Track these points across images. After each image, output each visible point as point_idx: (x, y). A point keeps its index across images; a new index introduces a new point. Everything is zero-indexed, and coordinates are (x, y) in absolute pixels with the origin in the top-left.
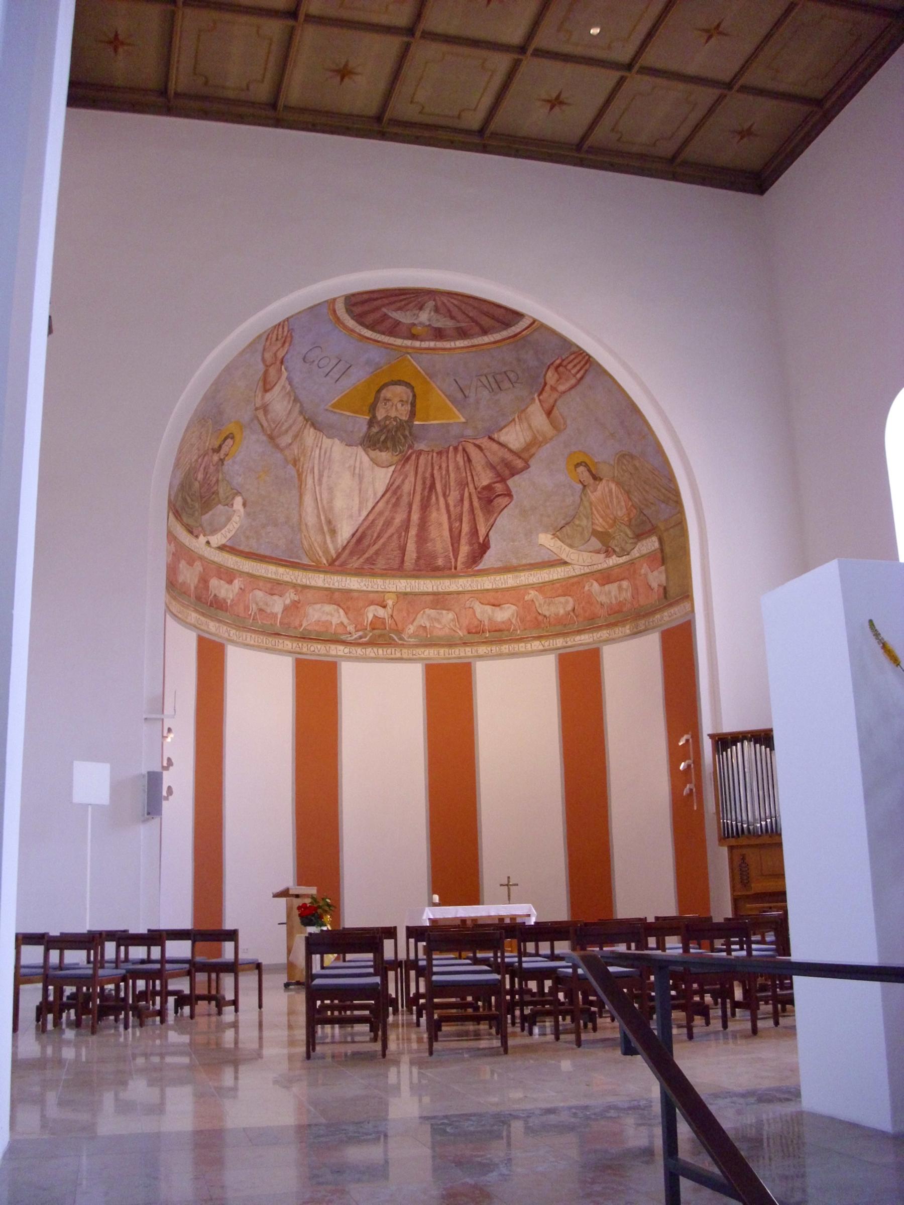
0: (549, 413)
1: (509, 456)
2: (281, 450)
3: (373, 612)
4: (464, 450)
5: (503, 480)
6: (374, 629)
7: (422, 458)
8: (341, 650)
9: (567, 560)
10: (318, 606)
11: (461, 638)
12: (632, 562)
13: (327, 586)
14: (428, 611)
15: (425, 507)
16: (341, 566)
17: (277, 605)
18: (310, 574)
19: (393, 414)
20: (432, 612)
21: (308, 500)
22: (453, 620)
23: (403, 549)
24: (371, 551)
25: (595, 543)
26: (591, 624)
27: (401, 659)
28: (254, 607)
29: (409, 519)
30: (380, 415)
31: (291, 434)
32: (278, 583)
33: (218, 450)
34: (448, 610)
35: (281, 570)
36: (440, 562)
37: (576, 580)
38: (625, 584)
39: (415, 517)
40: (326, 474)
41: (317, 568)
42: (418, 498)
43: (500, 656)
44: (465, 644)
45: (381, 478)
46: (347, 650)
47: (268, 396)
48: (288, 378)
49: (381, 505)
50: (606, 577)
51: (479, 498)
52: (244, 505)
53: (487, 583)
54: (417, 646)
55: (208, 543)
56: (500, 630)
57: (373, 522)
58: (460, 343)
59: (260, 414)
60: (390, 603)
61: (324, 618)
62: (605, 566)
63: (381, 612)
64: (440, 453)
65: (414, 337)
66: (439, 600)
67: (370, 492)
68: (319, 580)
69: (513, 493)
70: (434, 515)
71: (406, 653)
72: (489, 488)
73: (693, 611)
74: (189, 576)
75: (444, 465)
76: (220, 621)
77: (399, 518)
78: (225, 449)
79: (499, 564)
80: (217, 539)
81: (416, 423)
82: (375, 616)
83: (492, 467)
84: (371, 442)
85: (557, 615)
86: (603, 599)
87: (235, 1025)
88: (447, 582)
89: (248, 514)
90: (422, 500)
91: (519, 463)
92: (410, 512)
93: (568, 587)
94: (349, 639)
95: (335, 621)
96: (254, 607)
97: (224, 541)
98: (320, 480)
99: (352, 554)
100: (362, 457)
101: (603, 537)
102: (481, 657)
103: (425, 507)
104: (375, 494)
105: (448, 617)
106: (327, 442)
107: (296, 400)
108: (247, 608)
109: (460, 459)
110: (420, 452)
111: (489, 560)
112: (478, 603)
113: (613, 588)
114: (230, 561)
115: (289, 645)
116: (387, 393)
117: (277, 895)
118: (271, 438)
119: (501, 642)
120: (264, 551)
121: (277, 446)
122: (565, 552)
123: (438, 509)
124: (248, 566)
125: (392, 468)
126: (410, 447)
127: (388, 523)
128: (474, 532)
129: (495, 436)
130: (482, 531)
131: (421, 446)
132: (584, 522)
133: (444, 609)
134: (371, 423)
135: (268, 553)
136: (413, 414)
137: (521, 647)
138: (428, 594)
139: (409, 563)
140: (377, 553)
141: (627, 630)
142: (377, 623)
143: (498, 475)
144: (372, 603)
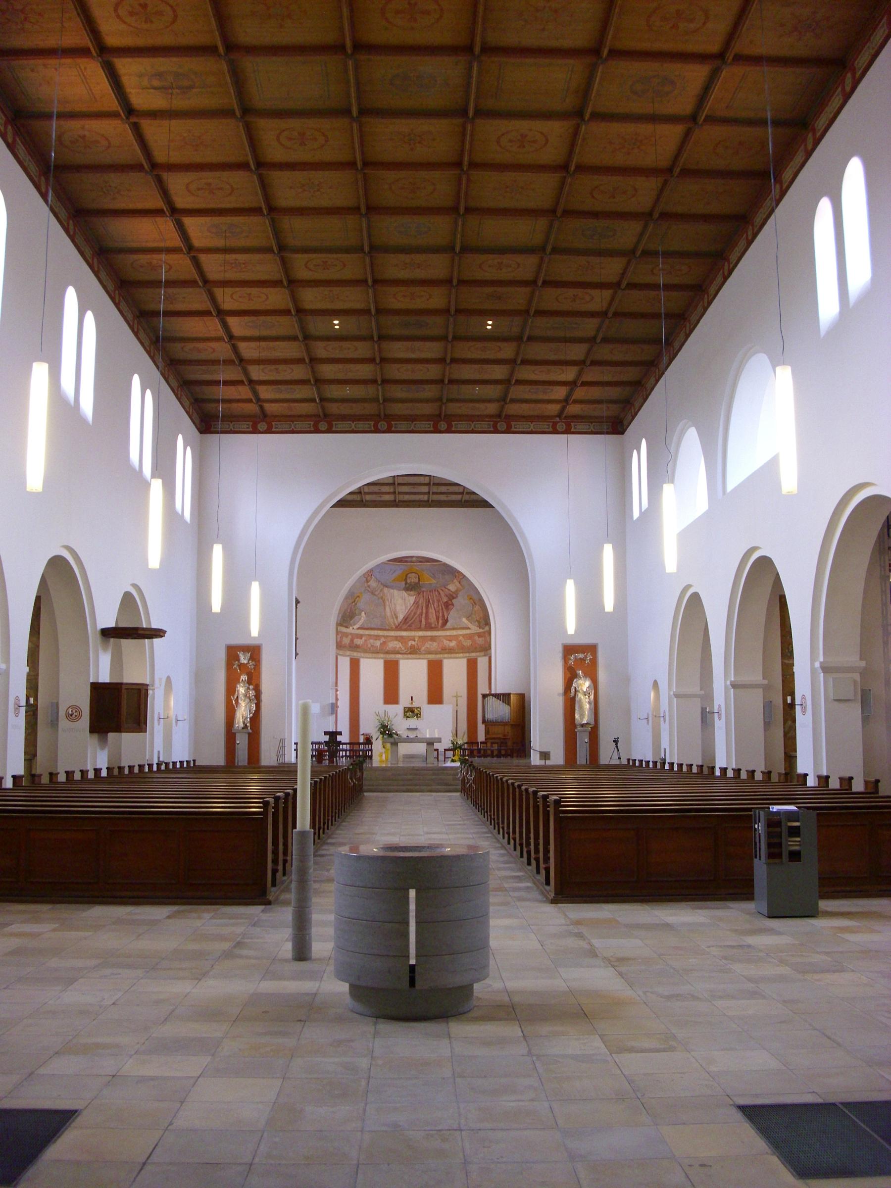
1: (451, 593)
3: (410, 643)
5: (451, 600)
8: (400, 656)
15: (427, 607)
17: (378, 643)
18: (390, 632)
19: (413, 581)
20: (429, 642)
21: (387, 609)
23: (421, 622)
24: (410, 622)
27: (420, 658)
28: (369, 645)
29: (422, 612)
30: (409, 581)
31: (379, 591)
35: (379, 632)
36: (433, 625)
38: (483, 638)
39: (424, 611)
41: (391, 629)
42: (424, 605)
43: (451, 658)
44: (441, 654)
45: (412, 599)
47: (369, 583)
49: (413, 607)
50: (479, 635)
52: (365, 614)
53: (448, 633)
54: (425, 654)
59: (368, 588)
60: (416, 640)
63: (414, 643)
64: (430, 592)
65: (413, 562)
66: (433, 639)
68: (392, 633)
71: (421, 656)
72: (446, 602)
74: (346, 641)
79: (451, 627)
80: (355, 627)
83: (447, 596)
84: (407, 589)
86: (478, 642)
91: (454, 596)
92: (422, 610)
93: (470, 637)
94: (403, 652)
95: (398, 646)
96: (369, 645)
99: (403, 624)
100: (404, 594)
101: (479, 622)
102: (445, 658)
103: (427, 607)
105: (435, 644)
106: (392, 591)
107: (379, 581)
109: (436, 592)
110: (423, 592)
111: (449, 625)
113: (481, 639)
114: (361, 632)
115: (382, 656)
116: (410, 575)
119: (452, 653)
120: (373, 626)
121: (375, 595)
122: (470, 625)
124: (367, 632)
125: (415, 597)
126: (420, 590)
127: (415, 614)
128: (443, 616)
130: (446, 617)
131: (424, 589)
132: (474, 617)
134: (406, 584)
136: (419, 580)
137: (457, 655)
140: (412, 623)
141: (482, 654)
142: (412, 647)
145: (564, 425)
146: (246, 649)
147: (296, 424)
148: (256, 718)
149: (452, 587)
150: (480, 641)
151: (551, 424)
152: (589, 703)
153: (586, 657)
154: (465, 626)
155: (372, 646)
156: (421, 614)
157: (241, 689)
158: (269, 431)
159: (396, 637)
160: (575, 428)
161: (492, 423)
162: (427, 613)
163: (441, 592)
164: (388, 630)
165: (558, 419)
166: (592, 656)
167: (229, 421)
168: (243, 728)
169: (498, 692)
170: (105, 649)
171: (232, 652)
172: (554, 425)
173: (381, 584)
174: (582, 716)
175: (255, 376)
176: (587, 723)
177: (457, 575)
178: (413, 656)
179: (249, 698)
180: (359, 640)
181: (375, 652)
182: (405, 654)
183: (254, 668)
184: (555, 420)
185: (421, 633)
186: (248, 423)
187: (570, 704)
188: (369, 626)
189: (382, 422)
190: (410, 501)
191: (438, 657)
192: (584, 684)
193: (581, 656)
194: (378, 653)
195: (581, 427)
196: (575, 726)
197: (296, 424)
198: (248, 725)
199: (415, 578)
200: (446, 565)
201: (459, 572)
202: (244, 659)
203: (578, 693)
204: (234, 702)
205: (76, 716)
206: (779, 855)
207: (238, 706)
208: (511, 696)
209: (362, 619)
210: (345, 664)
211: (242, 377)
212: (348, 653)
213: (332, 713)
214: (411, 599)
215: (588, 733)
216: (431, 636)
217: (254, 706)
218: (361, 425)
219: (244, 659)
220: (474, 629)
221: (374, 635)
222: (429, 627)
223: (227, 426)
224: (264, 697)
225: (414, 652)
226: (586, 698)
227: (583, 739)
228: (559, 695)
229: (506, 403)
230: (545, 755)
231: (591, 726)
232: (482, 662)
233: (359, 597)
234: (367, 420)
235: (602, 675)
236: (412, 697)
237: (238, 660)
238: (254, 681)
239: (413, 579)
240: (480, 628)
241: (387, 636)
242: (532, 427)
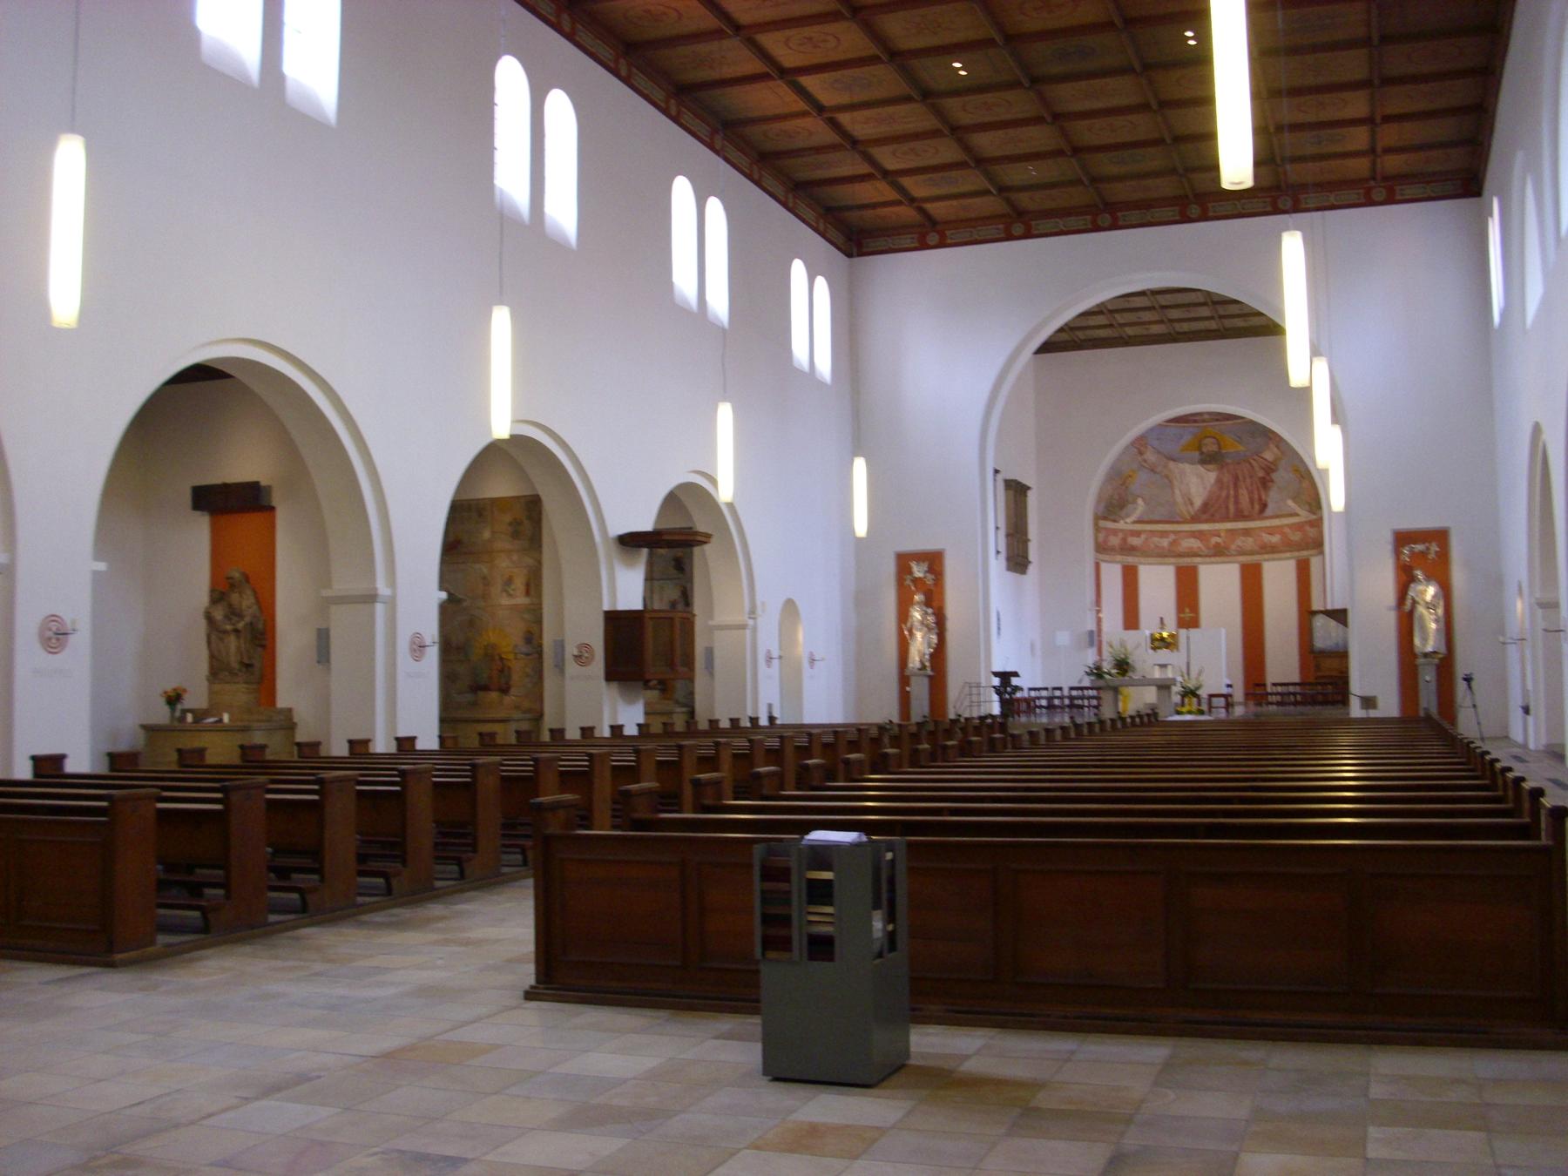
3: (1215, 540)
5: (1268, 474)
8: (1198, 560)
17: (1165, 543)
19: (1211, 449)
20: (1243, 538)
21: (1177, 492)
23: (1227, 508)
25: (1307, 507)
26: (1307, 548)
28: (1152, 546)
30: (1204, 450)
36: (1246, 513)
39: (1232, 492)
41: (1185, 522)
43: (1274, 559)
44: (1258, 553)
47: (1145, 457)
53: (1267, 523)
54: (1235, 555)
55: (1126, 523)
60: (1222, 534)
63: (1218, 540)
66: (1247, 532)
68: (1186, 527)
70: (1241, 491)
72: (1264, 478)
74: (1115, 541)
77: (1224, 493)
80: (1129, 520)
83: (1263, 469)
84: (1203, 462)
91: (1273, 467)
93: (1299, 527)
96: (1152, 546)
100: (1200, 469)
101: (1310, 504)
102: (1266, 560)
105: (1250, 540)
111: (1269, 512)
114: (1138, 527)
120: (1157, 518)
121: (1155, 473)
122: (1299, 510)
128: (1260, 499)
130: (1263, 497)
134: (1202, 453)
136: (1220, 448)
137: (1283, 555)
142: (1217, 544)
143: (1266, 471)
146: (920, 557)
148: (938, 656)
150: (1312, 532)
152: (1436, 621)
153: (1428, 549)
155: (1157, 546)
157: (917, 615)
158: (942, 244)
159: (1193, 532)
160: (1402, 195)
161: (1268, 200)
162: (1236, 497)
163: (1252, 461)
164: (1178, 522)
166: (1439, 546)
168: (920, 669)
170: (630, 564)
171: (904, 562)
172: (1368, 191)
174: (1425, 639)
175: (891, 164)
176: (1435, 652)
177: (1270, 435)
178: (1218, 559)
179: (927, 626)
180: (1135, 538)
181: (1161, 555)
182: (1206, 556)
187: (1407, 621)
188: (1152, 517)
190: (1194, 333)
191: (1255, 558)
194: (1166, 556)
195: (1410, 191)
196: (1415, 656)
198: (927, 664)
201: (1273, 432)
202: (918, 571)
203: (1418, 606)
205: (587, 658)
206: (784, 944)
209: (1140, 507)
210: (1112, 575)
211: (864, 169)
212: (1119, 558)
213: (1091, 644)
214: (1211, 476)
215: (1434, 667)
216: (1246, 529)
218: (1072, 222)
219: (918, 571)
220: (1304, 515)
222: (1240, 516)
225: (1219, 553)
226: (1430, 613)
227: (1428, 676)
230: (1369, 702)
231: (1440, 656)
232: (1315, 562)
233: (1130, 476)
235: (1458, 577)
236: (1162, 619)
237: (911, 573)
238: (934, 601)
239: (1209, 445)
242: (1332, 199)
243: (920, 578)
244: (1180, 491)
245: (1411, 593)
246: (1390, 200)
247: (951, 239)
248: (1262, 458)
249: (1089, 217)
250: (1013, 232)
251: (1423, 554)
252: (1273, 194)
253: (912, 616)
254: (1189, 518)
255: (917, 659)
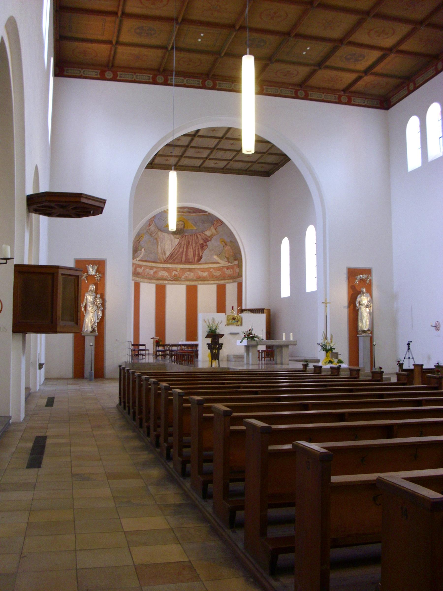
0: (216, 229)
1: (207, 237)
2: (153, 237)
3: (174, 273)
4: (197, 236)
5: (206, 242)
6: (175, 277)
7: (186, 237)
8: (166, 282)
9: (220, 262)
10: (161, 272)
11: (195, 279)
12: (233, 266)
13: (163, 267)
14: (187, 273)
15: (187, 248)
16: (167, 262)
20: (188, 273)
21: (159, 247)
22: (193, 275)
23: (182, 257)
24: (174, 258)
25: (226, 259)
26: (224, 279)
28: (146, 273)
29: (183, 251)
32: (152, 267)
33: (139, 240)
34: (192, 272)
35: (153, 264)
36: (191, 261)
37: (221, 267)
38: (232, 270)
39: (185, 250)
40: (164, 241)
41: (161, 263)
42: (185, 246)
44: (196, 281)
45: (177, 241)
46: (168, 282)
47: (150, 227)
48: (155, 223)
50: (228, 268)
51: (200, 246)
52: (144, 250)
54: (184, 281)
55: (136, 260)
56: (204, 278)
57: (175, 251)
58: (194, 214)
60: (178, 270)
61: (163, 274)
62: (228, 265)
63: (176, 273)
64: (191, 236)
66: (190, 270)
67: (174, 244)
68: (161, 265)
69: (208, 245)
71: (182, 283)
72: (202, 244)
73: (242, 280)
75: (192, 238)
76: (138, 277)
77: (181, 250)
78: (140, 239)
79: (205, 262)
80: (138, 259)
81: (185, 229)
82: (175, 274)
83: (203, 239)
85: (217, 275)
86: (227, 273)
87: (145, 359)
88: (192, 266)
89: (145, 252)
90: (186, 246)
91: (209, 239)
93: (220, 269)
94: (169, 279)
95: (165, 275)
96: (146, 273)
97: (140, 259)
98: (162, 242)
99: (170, 259)
101: (228, 258)
103: (187, 248)
104: (175, 245)
106: (164, 234)
107: (156, 226)
108: (145, 274)
109: (195, 237)
110: (186, 236)
111: (202, 261)
112: (199, 271)
113: (229, 270)
114: (141, 263)
115: (154, 281)
117: (152, 339)
118: (151, 235)
119: (204, 281)
120: (149, 260)
121: (152, 236)
122: (219, 261)
123: (190, 248)
124: (145, 264)
125: (179, 239)
127: (178, 252)
128: (199, 254)
129: (204, 232)
130: (201, 254)
131: (186, 234)
133: (191, 272)
135: (149, 260)
138: (188, 268)
139: (183, 261)
140: (176, 258)
141: (231, 281)
142: (175, 275)
143: (204, 241)
144: (174, 270)
145: (346, 97)
146: (93, 262)
147: (137, 76)
148: (101, 323)
149: (208, 233)
150: (228, 272)
151: (337, 96)
153: (368, 276)
154: (215, 261)
155: (148, 274)
156: (183, 251)
158: (114, 79)
160: (354, 102)
163: (199, 236)
165: (342, 93)
167: (79, 68)
168: (91, 332)
169: (248, 307)
172: (340, 97)
173: (158, 228)
178: (176, 282)
179: (97, 305)
180: (140, 269)
181: (150, 278)
183: (100, 280)
184: (340, 94)
185: (182, 266)
186: (97, 71)
188: (146, 259)
189: (209, 81)
192: (364, 299)
193: (365, 276)
194: (152, 279)
195: (358, 101)
197: (137, 76)
198: (96, 329)
199: (182, 225)
200: (210, 215)
204: (83, 309)
207: (87, 312)
208: (265, 310)
216: (189, 268)
217: (100, 312)
218: (192, 81)
220: (223, 263)
221: (149, 266)
222: (188, 262)
223: (79, 72)
224: (108, 305)
225: (176, 279)
227: (363, 344)
228: (344, 307)
229: (320, 68)
234: (197, 78)
236: (233, 307)
240: (229, 262)
241: (158, 267)
242: (323, 97)
243: (91, 275)
244: (161, 247)
245: (358, 299)
246: (349, 103)
247: (120, 77)
248: (204, 234)
249: (201, 80)
250: (157, 80)
251: (363, 281)
252: (296, 88)
253: (87, 299)
254: (163, 261)
255: (90, 325)
